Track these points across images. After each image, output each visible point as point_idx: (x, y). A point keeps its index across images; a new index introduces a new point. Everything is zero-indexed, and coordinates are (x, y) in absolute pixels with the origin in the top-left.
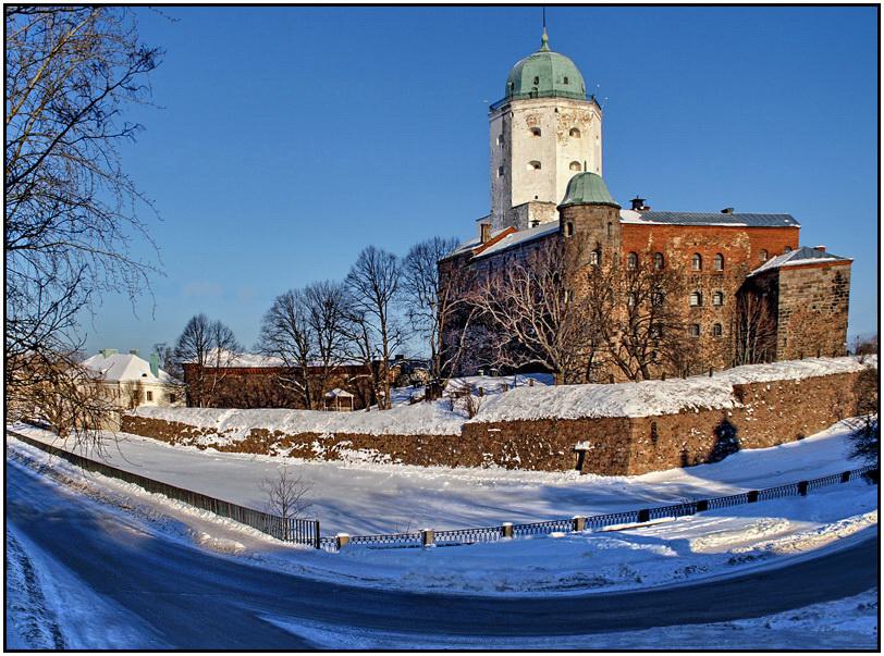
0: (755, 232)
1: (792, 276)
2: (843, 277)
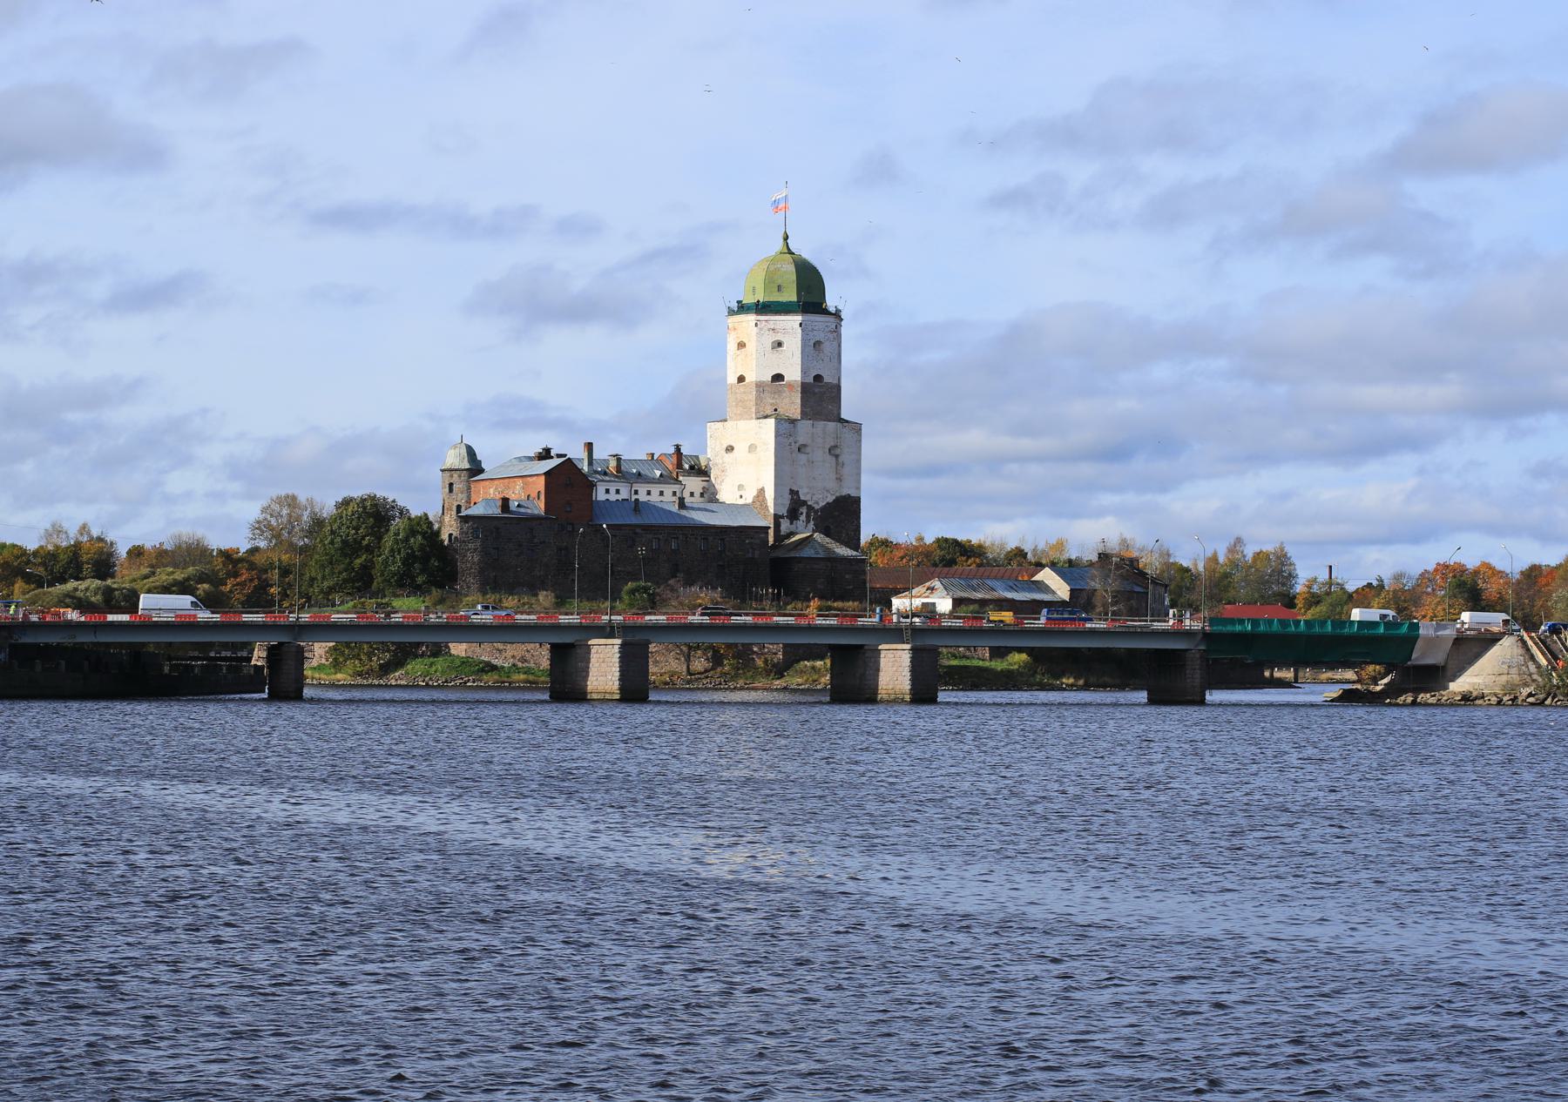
0: (525, 479)
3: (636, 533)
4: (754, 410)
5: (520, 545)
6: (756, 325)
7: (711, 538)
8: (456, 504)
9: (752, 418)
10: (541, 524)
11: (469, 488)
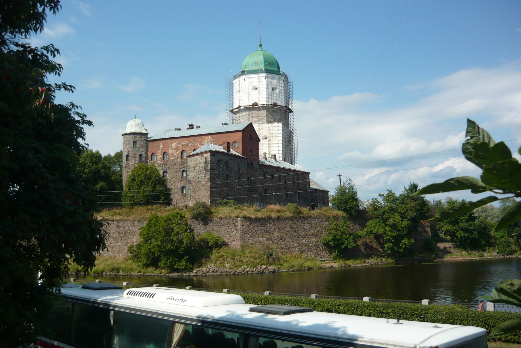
1: (191, 161)
2: (207, 160)
3: (274, 171)
4: (265, 119)
5: (236, 174)
6: (265, 78)
7: (295, 178)
8: (138, 154)
9: (264, 123)
10: (242, 162)
11: (147, 146)
